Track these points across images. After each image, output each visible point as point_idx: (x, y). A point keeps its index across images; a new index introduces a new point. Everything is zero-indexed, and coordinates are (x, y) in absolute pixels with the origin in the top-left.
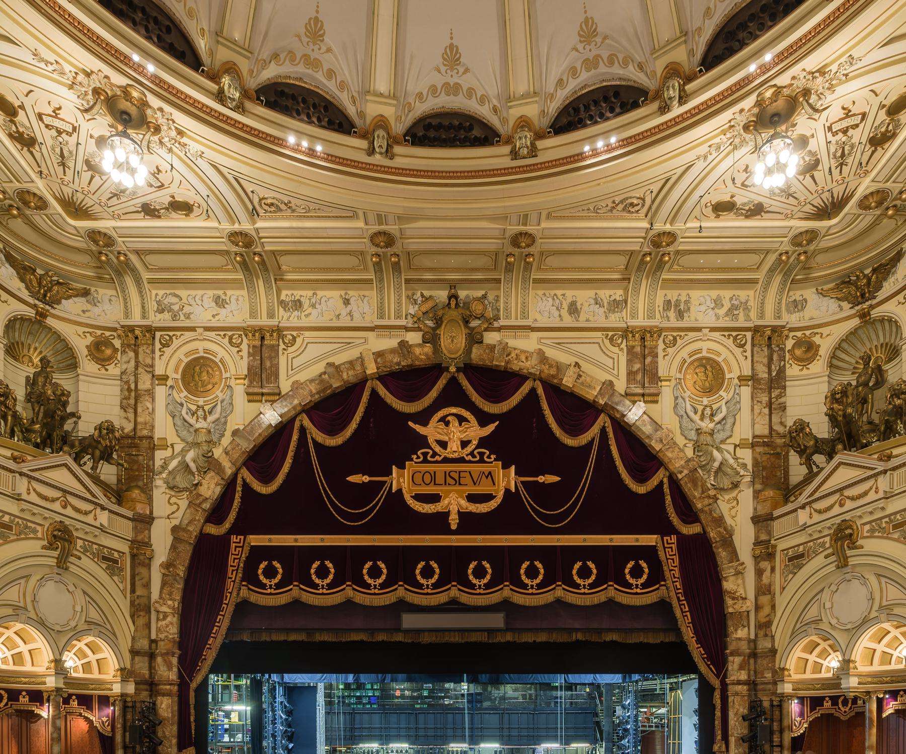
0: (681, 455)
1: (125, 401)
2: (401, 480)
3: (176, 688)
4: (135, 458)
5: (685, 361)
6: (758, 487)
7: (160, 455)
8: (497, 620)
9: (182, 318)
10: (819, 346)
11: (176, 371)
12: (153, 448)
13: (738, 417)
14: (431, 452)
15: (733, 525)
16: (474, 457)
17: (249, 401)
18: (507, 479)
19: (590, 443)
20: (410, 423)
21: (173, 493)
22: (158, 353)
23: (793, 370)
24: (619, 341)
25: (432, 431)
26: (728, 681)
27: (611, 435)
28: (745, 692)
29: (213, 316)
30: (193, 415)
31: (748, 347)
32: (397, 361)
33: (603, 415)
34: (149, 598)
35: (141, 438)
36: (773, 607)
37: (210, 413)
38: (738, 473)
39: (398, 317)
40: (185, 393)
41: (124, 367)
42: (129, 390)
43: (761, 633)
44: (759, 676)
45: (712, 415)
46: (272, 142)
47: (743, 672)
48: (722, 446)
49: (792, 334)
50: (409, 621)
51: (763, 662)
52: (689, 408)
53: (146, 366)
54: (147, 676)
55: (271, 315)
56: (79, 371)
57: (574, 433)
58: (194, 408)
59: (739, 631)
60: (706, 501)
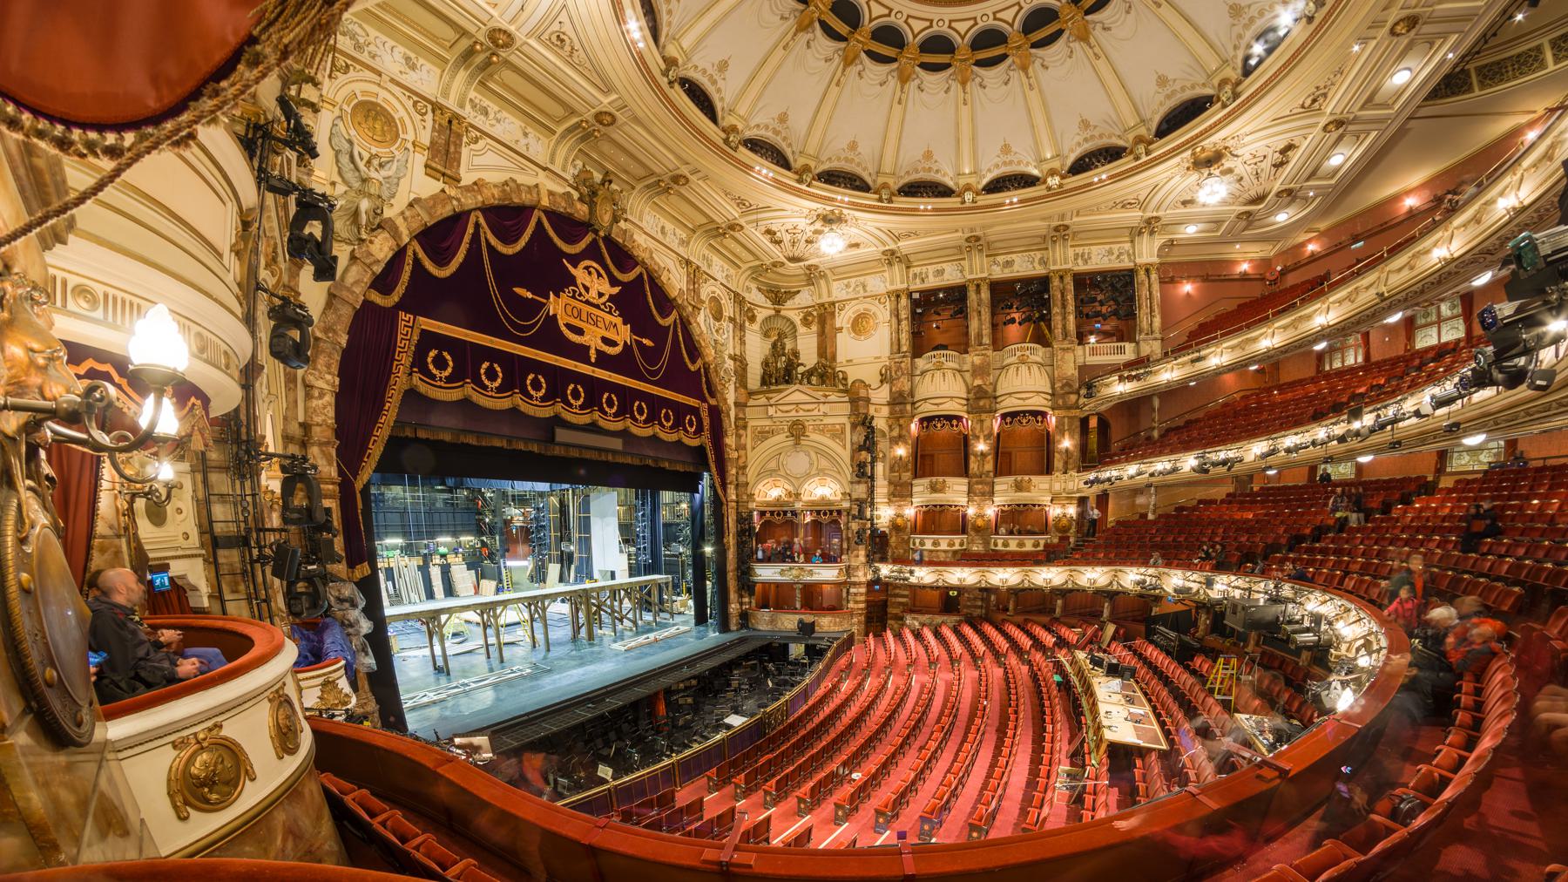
8: (617, 444)
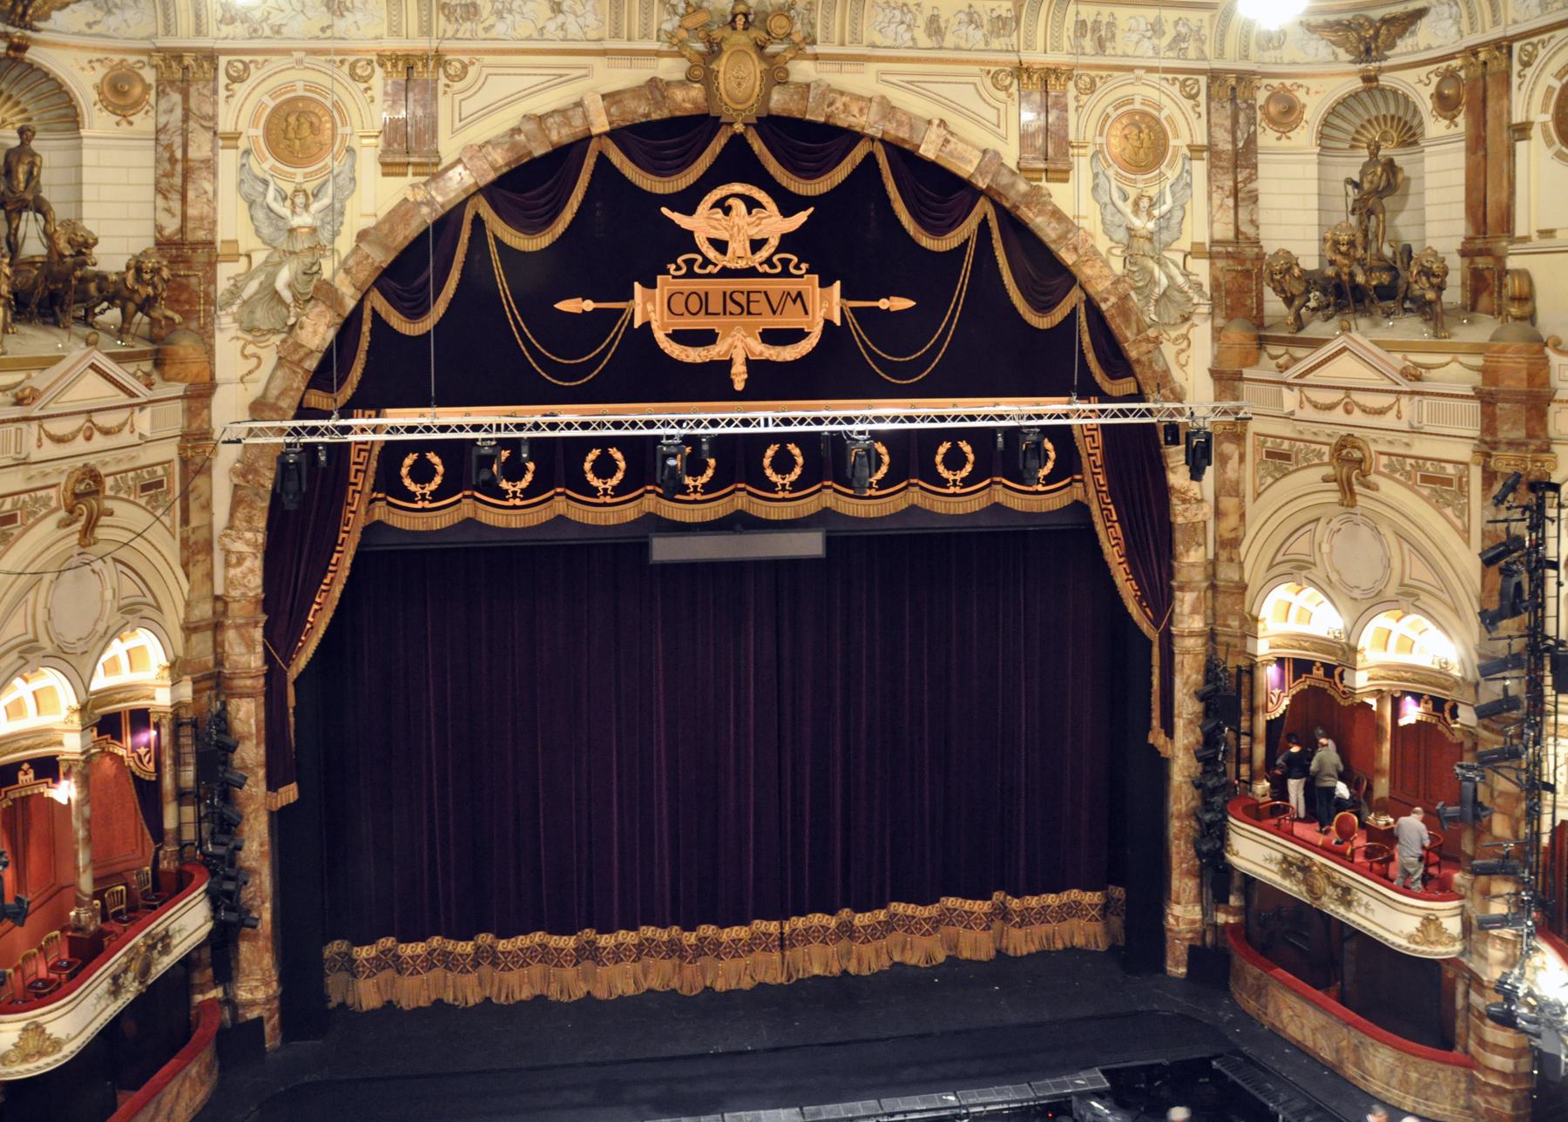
0: (1106, 271)
1: (164, 180)
2: (650, 307)
3: (262, 681)
4: (184, 281)
5: (1108, 116)
6: (1220, 322)
7: (226, 273)
8: (811, 545)
9: (268, 32)
10: (1304, 106)
11: (254, 124)
12: (212, 265)
13: (1188, 207)
14: (700, 259)
15: (1184, 384)
16: (773, 266)
17: (384, 174)
18: (827, 304)
19: (964, 245)
20: (665, 210)
21: (249, 338)
22: (222, 93)
23: (1267, 138)
24: (1007, 82)
25: (701, 223)
26: (1174, 630)
27: (996, 235)
28: (1200, 649)
29: (323, 30)
30: (285, 199)
31: (1202, 98)
32: (641, 110)
33: (982, 199)
34: (210, 525)
35: (194, 246)
36: (1242, 516)
37: (315, 196)
38: (1190, 300)
39: (645, 36)
40: (271, 161)
41: (163, 120)
42: (172, 160)
43: (1224, 555)
44: (1220, 621)
45: (1152, 205)
47: (1197, 617)
48: (1166, 254)
49: (1265, 81)
50: (664, 549)
51: (1225, 601)
52: (1116, 195)
53: (204, 118)
54: (211, 664)
55: (426, 31)
56: (83, 132)
57: (938, 231)
58: (289, 188)
59: (1192, 553)
60: (1145, 347)
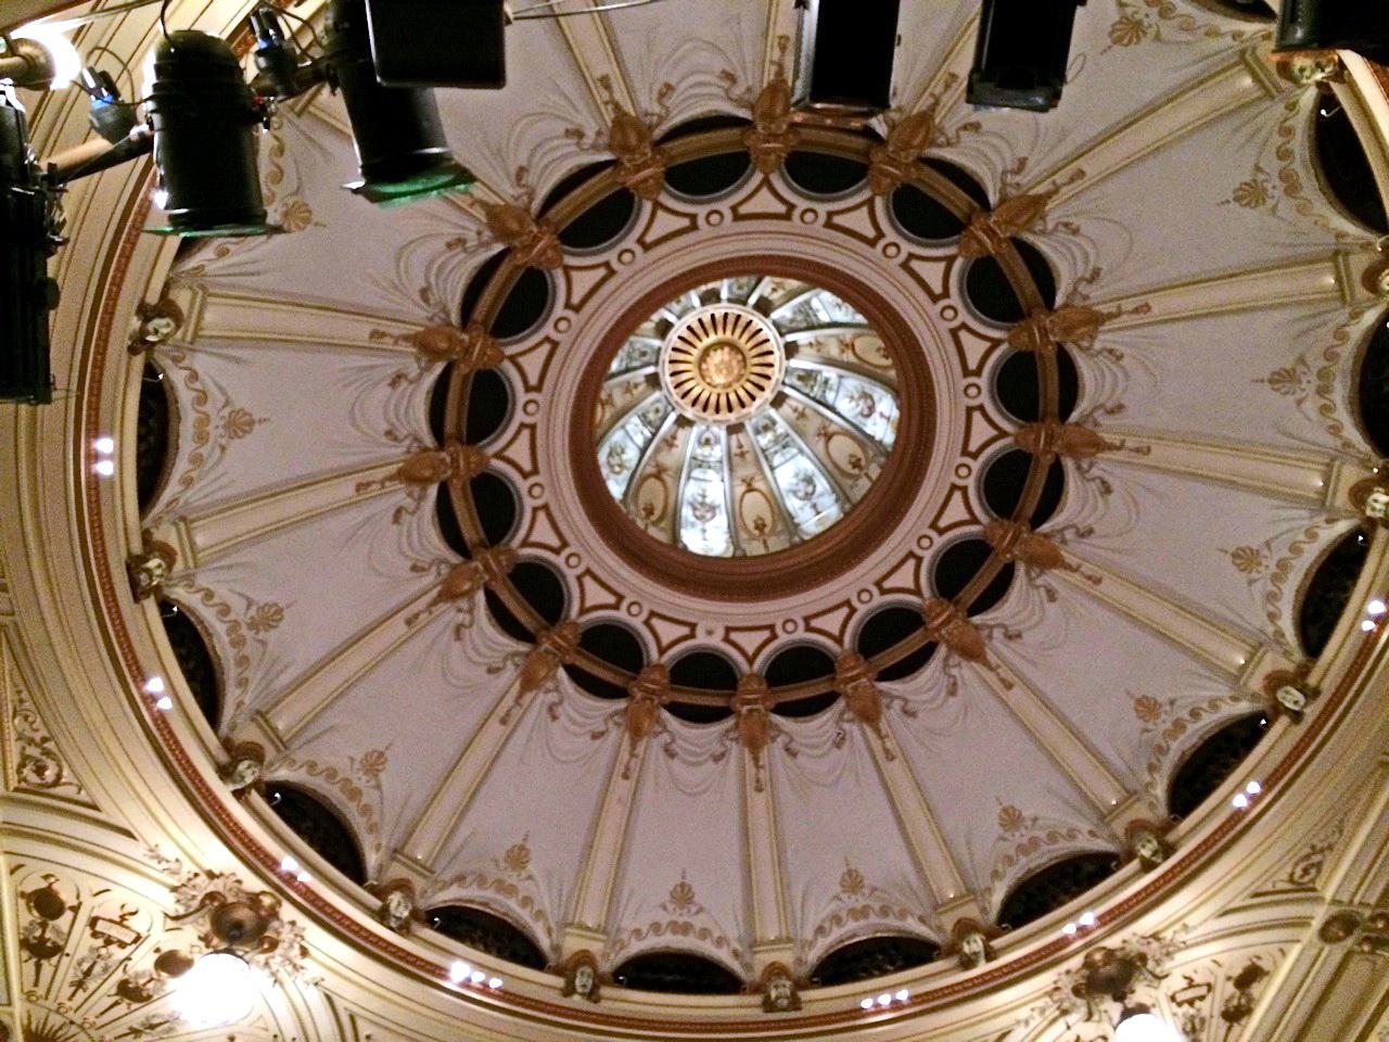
46: (433, 973)
